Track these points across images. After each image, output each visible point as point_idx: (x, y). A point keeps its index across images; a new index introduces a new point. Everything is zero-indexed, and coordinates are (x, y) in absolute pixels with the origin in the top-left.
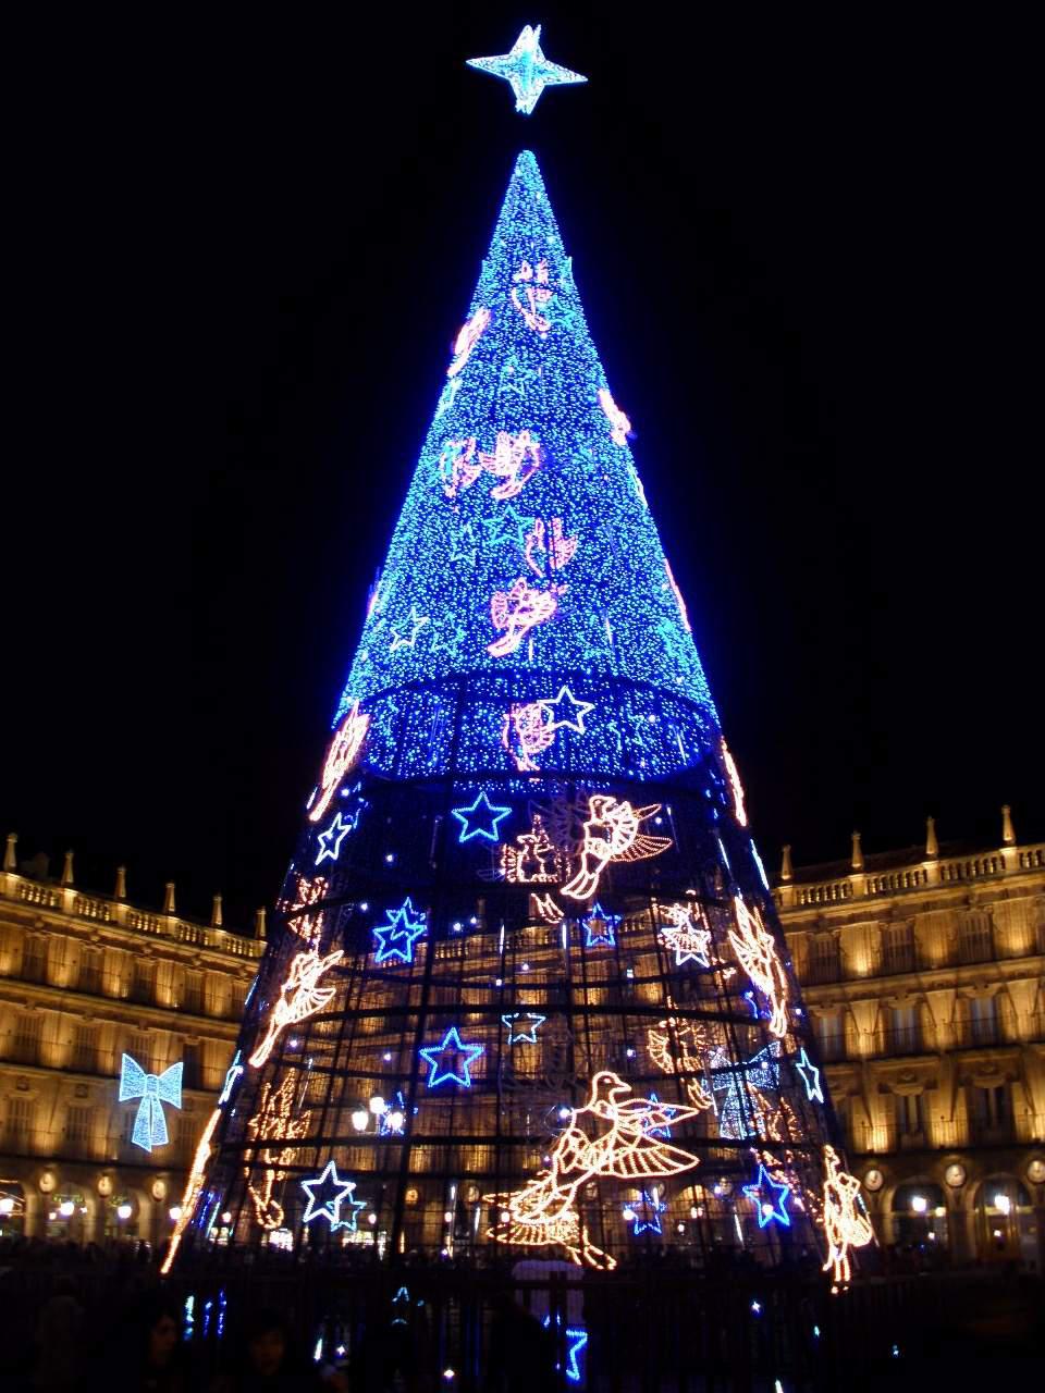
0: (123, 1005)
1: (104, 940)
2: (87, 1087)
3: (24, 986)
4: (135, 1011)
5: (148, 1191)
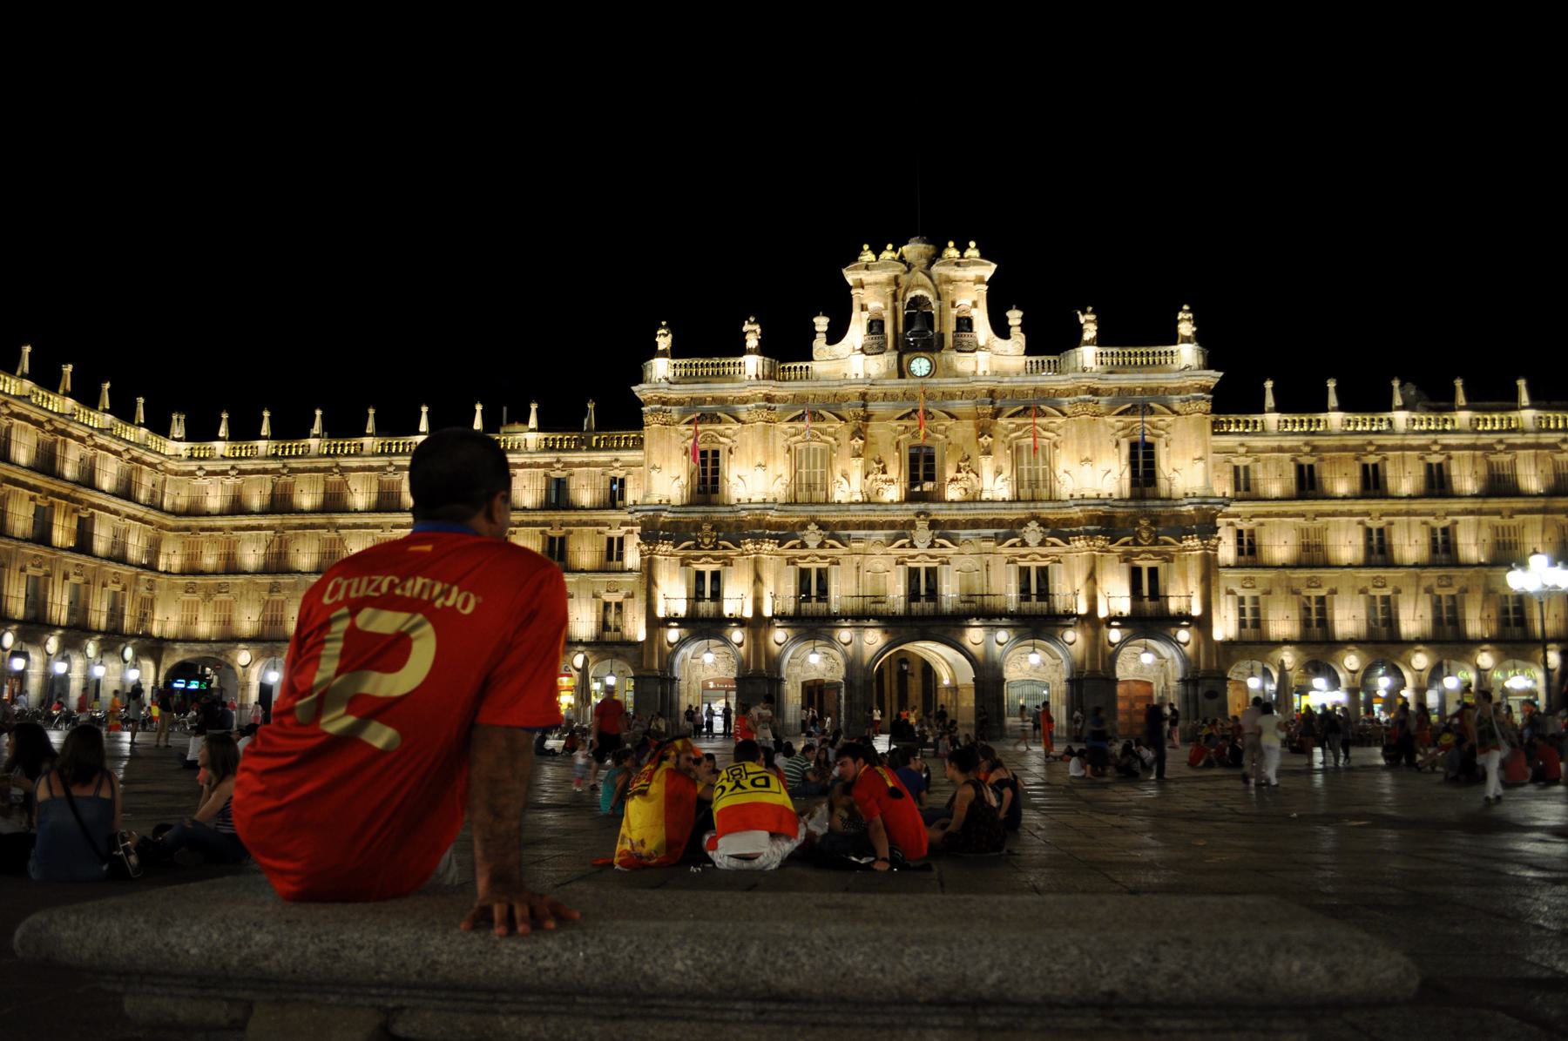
0: (1480, 500)
2: (1449, 577)
4: (1493, 503)
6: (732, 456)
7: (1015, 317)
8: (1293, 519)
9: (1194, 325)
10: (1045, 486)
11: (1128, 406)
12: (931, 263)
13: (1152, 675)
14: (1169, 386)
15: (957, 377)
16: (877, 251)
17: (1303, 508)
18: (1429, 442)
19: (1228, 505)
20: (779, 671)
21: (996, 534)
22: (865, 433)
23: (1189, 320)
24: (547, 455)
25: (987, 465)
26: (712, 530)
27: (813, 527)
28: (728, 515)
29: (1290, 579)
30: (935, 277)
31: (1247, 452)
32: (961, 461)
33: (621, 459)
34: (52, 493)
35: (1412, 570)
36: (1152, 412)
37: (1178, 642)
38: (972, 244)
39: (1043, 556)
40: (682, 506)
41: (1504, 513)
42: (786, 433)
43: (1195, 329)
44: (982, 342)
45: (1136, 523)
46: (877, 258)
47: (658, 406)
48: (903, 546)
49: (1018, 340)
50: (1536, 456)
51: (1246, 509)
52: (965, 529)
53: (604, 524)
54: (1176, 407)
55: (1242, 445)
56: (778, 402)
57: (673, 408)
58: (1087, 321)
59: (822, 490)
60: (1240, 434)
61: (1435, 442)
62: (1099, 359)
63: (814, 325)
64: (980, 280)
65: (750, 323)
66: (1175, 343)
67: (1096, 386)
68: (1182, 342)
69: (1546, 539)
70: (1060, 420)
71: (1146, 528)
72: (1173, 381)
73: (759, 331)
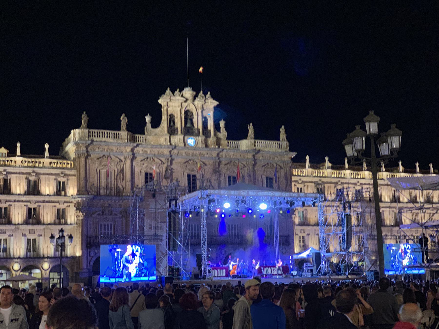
7: (222, 124)
16: (173, 91)
24: (29, 169)
38: (209, 93)
49: (223, 134)
53: (58, 202)
55: (300, 180)
63: (145, 119)
69: (391, 217)
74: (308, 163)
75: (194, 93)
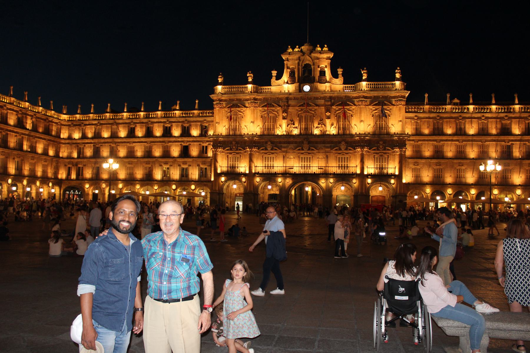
0: (497, 137)
1: (487, 118)
3: (456, 136)
4: (502, 138)
5: (515, 193)
6: (243, 119)
7: (340, 71)
8: (432, 142)
9: (401, 75)
10: (348, 130)
11: (377, 102)
12: (311, 52)
13: (385, 194)
14: (391, 95)
15: (319, 92)
16: (293, 49)
17: (436, 138)
18: (481, 116)
19: (410, 137)
20: (258, 192)
21: (331, 146)
22: (287, 111)
23: (399, 73)
25: (328, 122)
26: (236, 144)
27: (269, 143)
28: (240, 139)
29: (430, 162)
30: (313, 57)
31: (418, 119)
32: (320, 121)
33: (207, 119)
34: (23, 134)
35: (472, 160)
36: (385, 105)
37: (391, 183)
38: (326, 46)
39: (346, 153)
40: (226, 136)
41: (506, 141)
42: (261, 111)
43: (401, 76)
44: (328, 79)
45: (378, 143)
46: (293, 50)
47: (218, 102)
48: (299, 150)
50: (519, 121)
51: (417, 138)
52: (320, 144)
54: (394, 103)
56: (259, 100)
57: (223, 102)
58: (364, 73)
59: (273, 130)
60: (415, 112)
61: (483, 116)
62: (367, 86)
63: (272, 73)
64: (328, 58)
65: (249, 73)
66: (394, 81)
67: (366, 95)
68: (397, 81)
70: (354, 107)
71: (381, 145)
72: (393, 94)
73: (252, 76)
74: (426, 100)
75: (311, 47)
